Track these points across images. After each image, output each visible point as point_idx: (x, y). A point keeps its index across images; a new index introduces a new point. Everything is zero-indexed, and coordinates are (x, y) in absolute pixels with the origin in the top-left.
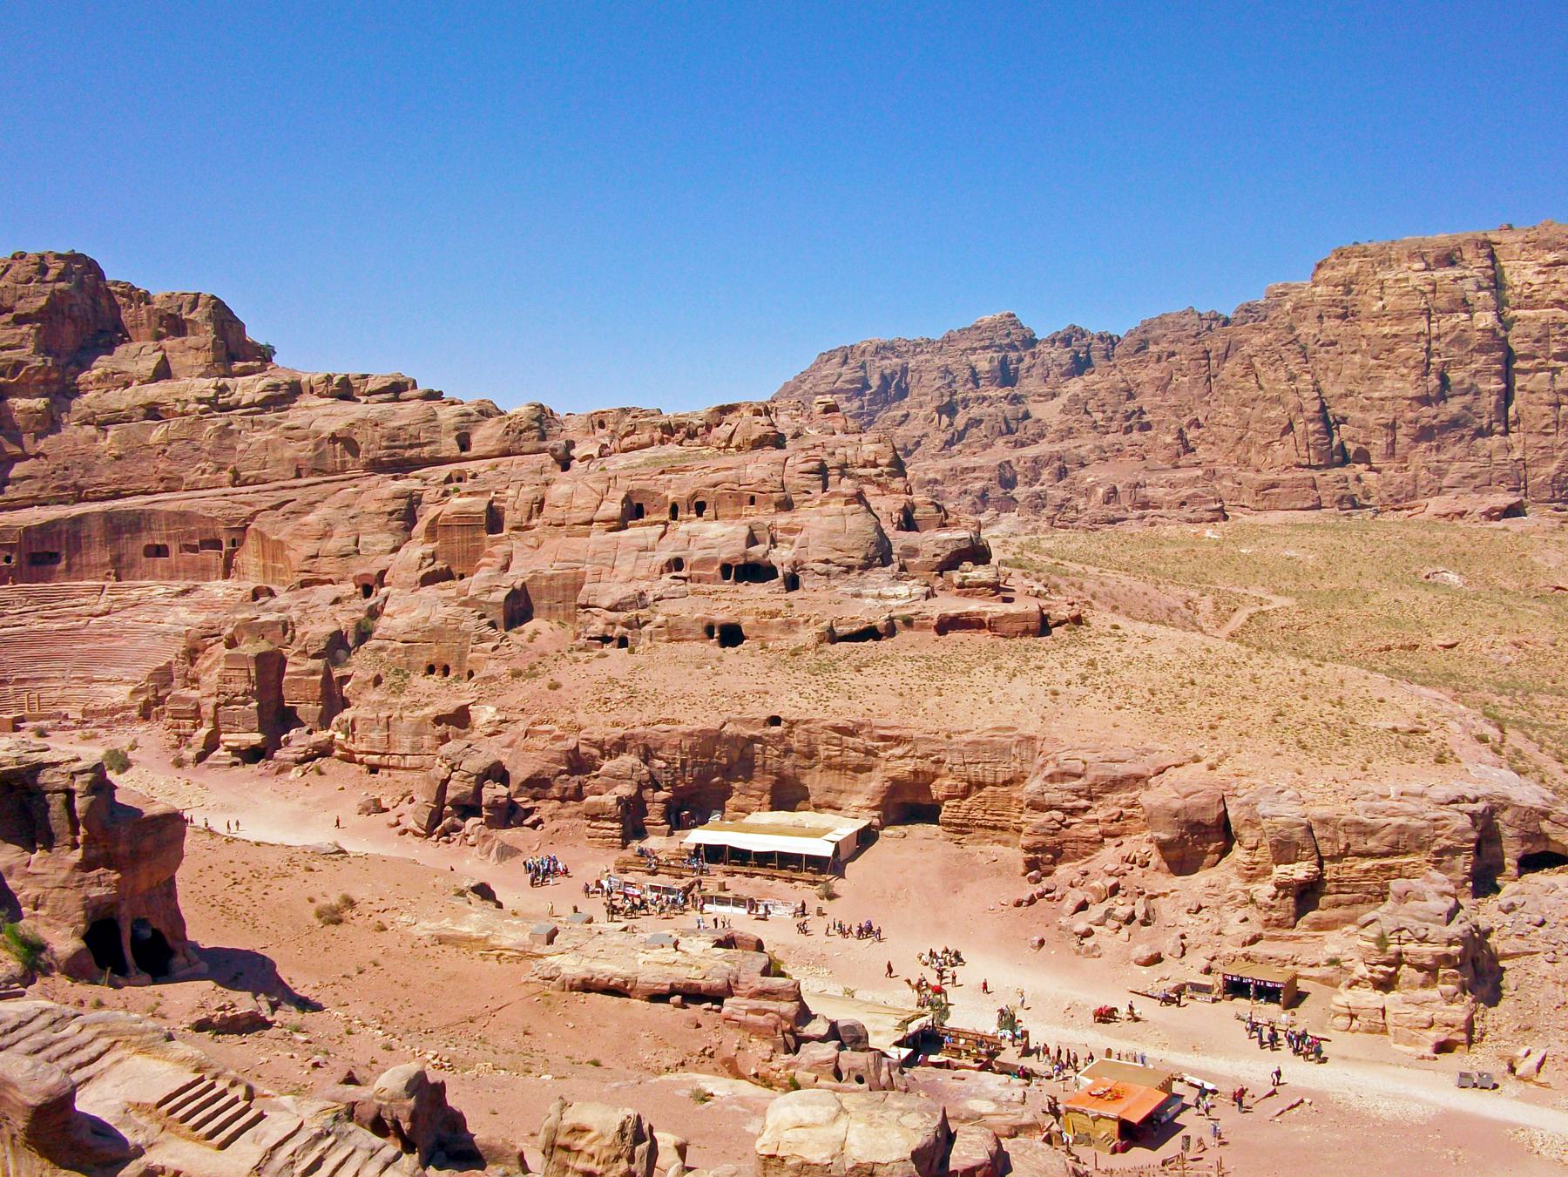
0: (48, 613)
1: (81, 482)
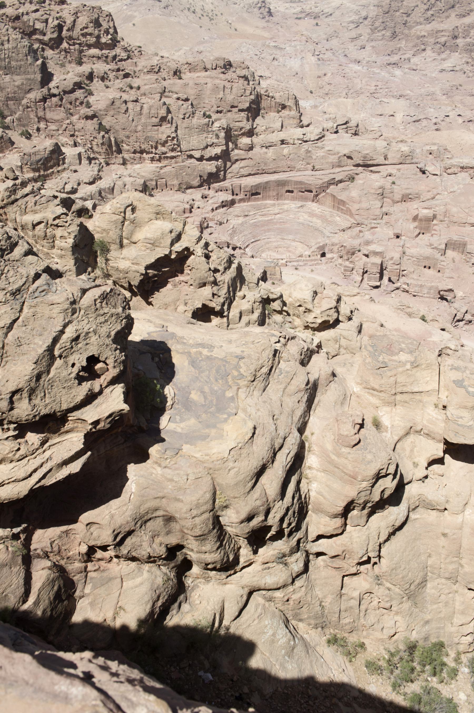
1: (264, 168)
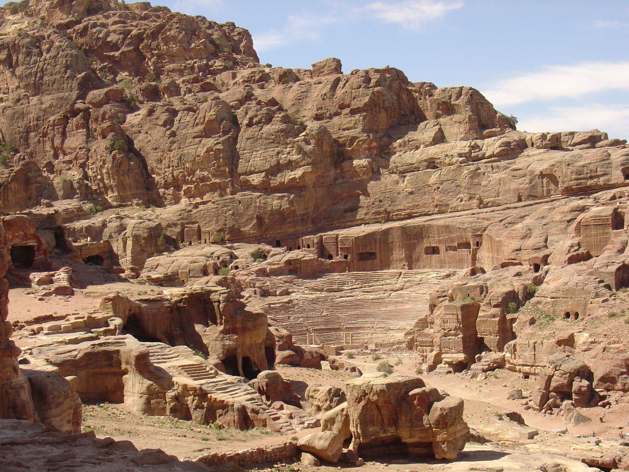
0: (367, 289)
1: (389, 209)
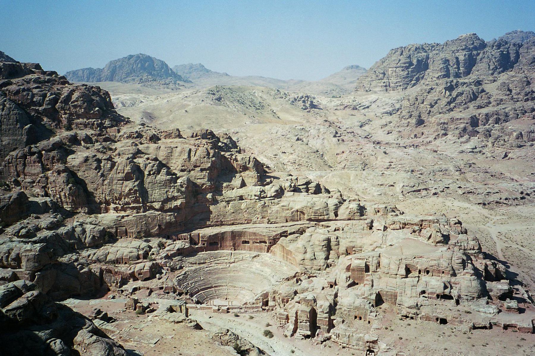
1: (223, 220)
